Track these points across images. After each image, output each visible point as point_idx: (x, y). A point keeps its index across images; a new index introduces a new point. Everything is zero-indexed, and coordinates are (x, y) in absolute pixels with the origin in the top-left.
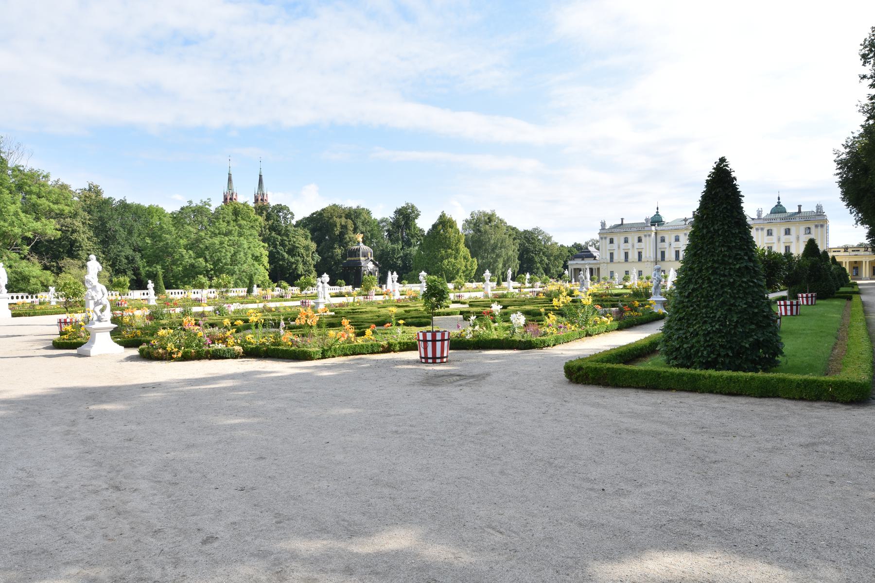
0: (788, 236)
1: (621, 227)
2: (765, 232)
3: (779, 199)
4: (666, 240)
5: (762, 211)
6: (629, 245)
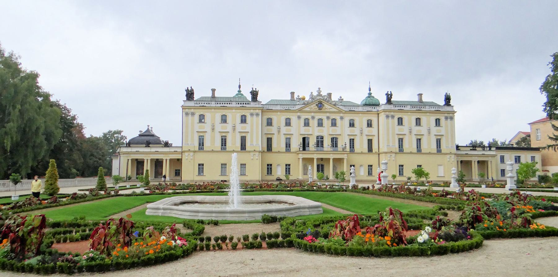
2: (396, 120)
3: (370, 90)
4: (274, 122)
5: (391, 95)
6: (228, 127)
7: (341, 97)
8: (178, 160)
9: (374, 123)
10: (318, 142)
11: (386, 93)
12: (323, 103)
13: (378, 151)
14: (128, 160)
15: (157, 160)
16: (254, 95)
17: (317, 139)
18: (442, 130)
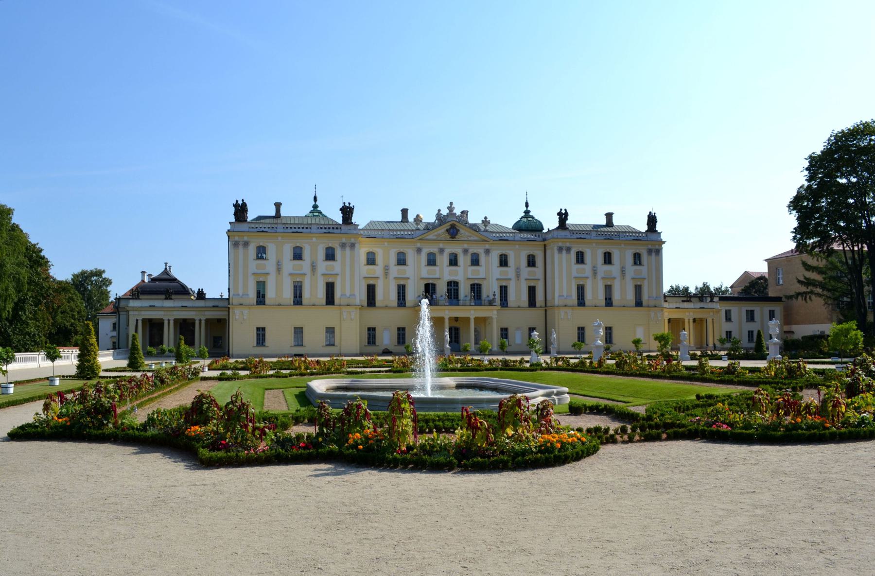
0: (607, 267)
1: (279, 221)
2: (573, 256)
5: (566, 214)
6: (305, 265)
7: (486, 218)
8: (218, 321)
9: (539, 261)
10: (449, 291)
11: (559, 211)
12: (457, 228)
13: (543, 305)
14: (137, 320)
15: (184, 320)
16: (347, 212)
17: (448, 286)
18: (643, 270)
